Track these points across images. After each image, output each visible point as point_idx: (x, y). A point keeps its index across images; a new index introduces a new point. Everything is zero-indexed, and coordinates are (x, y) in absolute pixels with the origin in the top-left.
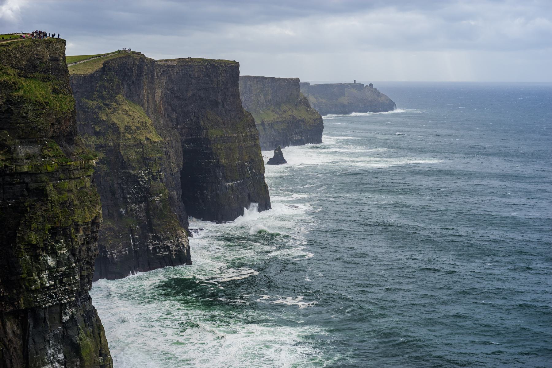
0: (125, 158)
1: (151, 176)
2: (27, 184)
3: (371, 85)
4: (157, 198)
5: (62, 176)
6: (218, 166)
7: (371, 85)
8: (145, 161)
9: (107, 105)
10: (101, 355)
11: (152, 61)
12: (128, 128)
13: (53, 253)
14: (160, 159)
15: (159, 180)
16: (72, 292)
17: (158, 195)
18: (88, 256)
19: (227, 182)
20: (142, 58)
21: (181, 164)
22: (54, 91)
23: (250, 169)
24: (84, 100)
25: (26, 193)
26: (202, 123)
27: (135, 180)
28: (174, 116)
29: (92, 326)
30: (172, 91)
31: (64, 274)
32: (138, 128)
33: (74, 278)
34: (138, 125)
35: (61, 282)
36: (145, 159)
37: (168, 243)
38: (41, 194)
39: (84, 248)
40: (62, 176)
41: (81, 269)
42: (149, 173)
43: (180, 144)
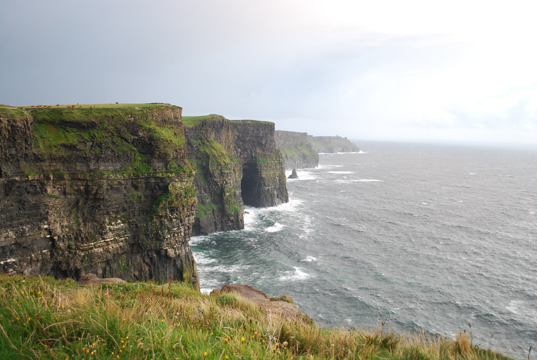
0: (212, 171)
2: (158, 183)
3: (346, 138)
4: (227, 194)
5: (177, 180)
6: (262, 178)
7: (346, 138)
8: (222, 174)
9: (204, 143)
10: (193, 276)
11: (228, 120)
12: (214, 156)
14: (230, 173)
16: (180, 242)
18: (189, 223)
20: (223, 119)
21: (242, 176)
22: (175, 134)
25: (157, 188)
27: (216, 184)
28: (239, 150)
29: (189, 260)
30: (238, 137)
32: (219, 156)
33: (181, 235)
34: (220, 154)
35: (174, 235)
36: (222, 173)
37: (232, 218)
38: (166, 189)
39: (187, 219)
40: (177, 180)
41: (185, 230)
43: (241, 165)
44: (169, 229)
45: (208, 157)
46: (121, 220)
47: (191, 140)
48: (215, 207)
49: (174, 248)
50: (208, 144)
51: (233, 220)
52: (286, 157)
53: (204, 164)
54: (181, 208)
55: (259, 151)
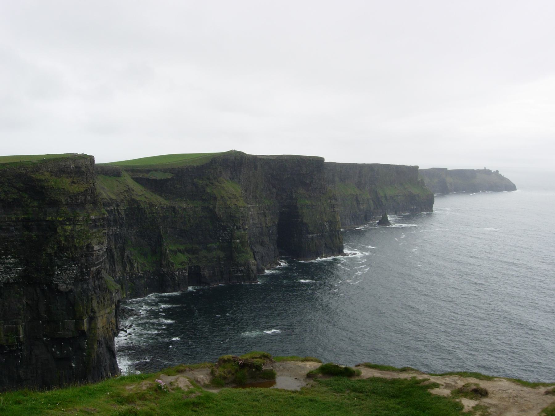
1: (235, 227)
3: (497, 171)
4: (238, 241)
5: (68, 223)
7: (497, 171)
9: (212, 184)
12: (222, 198)
13: (60, 258)
15: (242, 230)
17: (239, 239)
19: (309, 234)
23: (329, 226)
24: (195, 180)
26: (294, 196)
31: (67, 269)
32: (230, 198)
37: (242, 268)
40: (68, 223)
42: (234, 225)
44: (59, 267)
45: (215, 198)
46: (11, 255)
47: (195, 180)
48: (222, 255)
49: (65, 283)
50: (217, 183)
51: (242, 270)
52: (385, 197)
53: (211, 207)
54: (73, 249)
55: (301, 191)
